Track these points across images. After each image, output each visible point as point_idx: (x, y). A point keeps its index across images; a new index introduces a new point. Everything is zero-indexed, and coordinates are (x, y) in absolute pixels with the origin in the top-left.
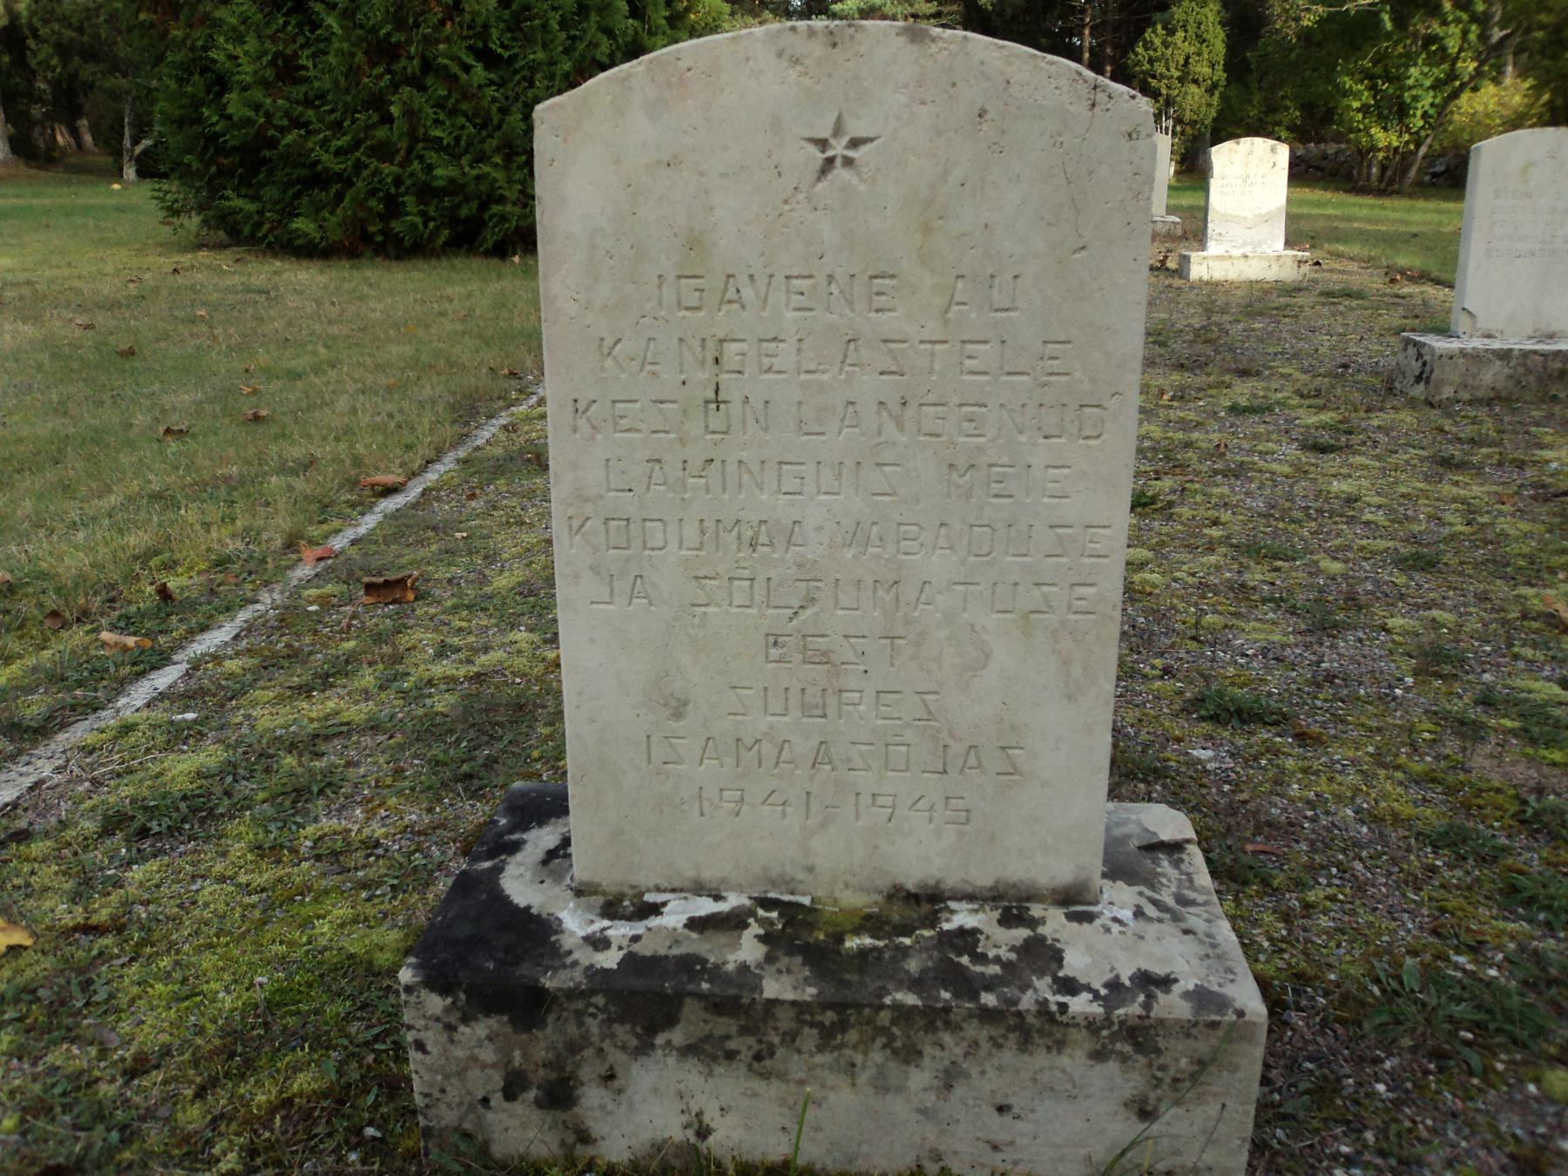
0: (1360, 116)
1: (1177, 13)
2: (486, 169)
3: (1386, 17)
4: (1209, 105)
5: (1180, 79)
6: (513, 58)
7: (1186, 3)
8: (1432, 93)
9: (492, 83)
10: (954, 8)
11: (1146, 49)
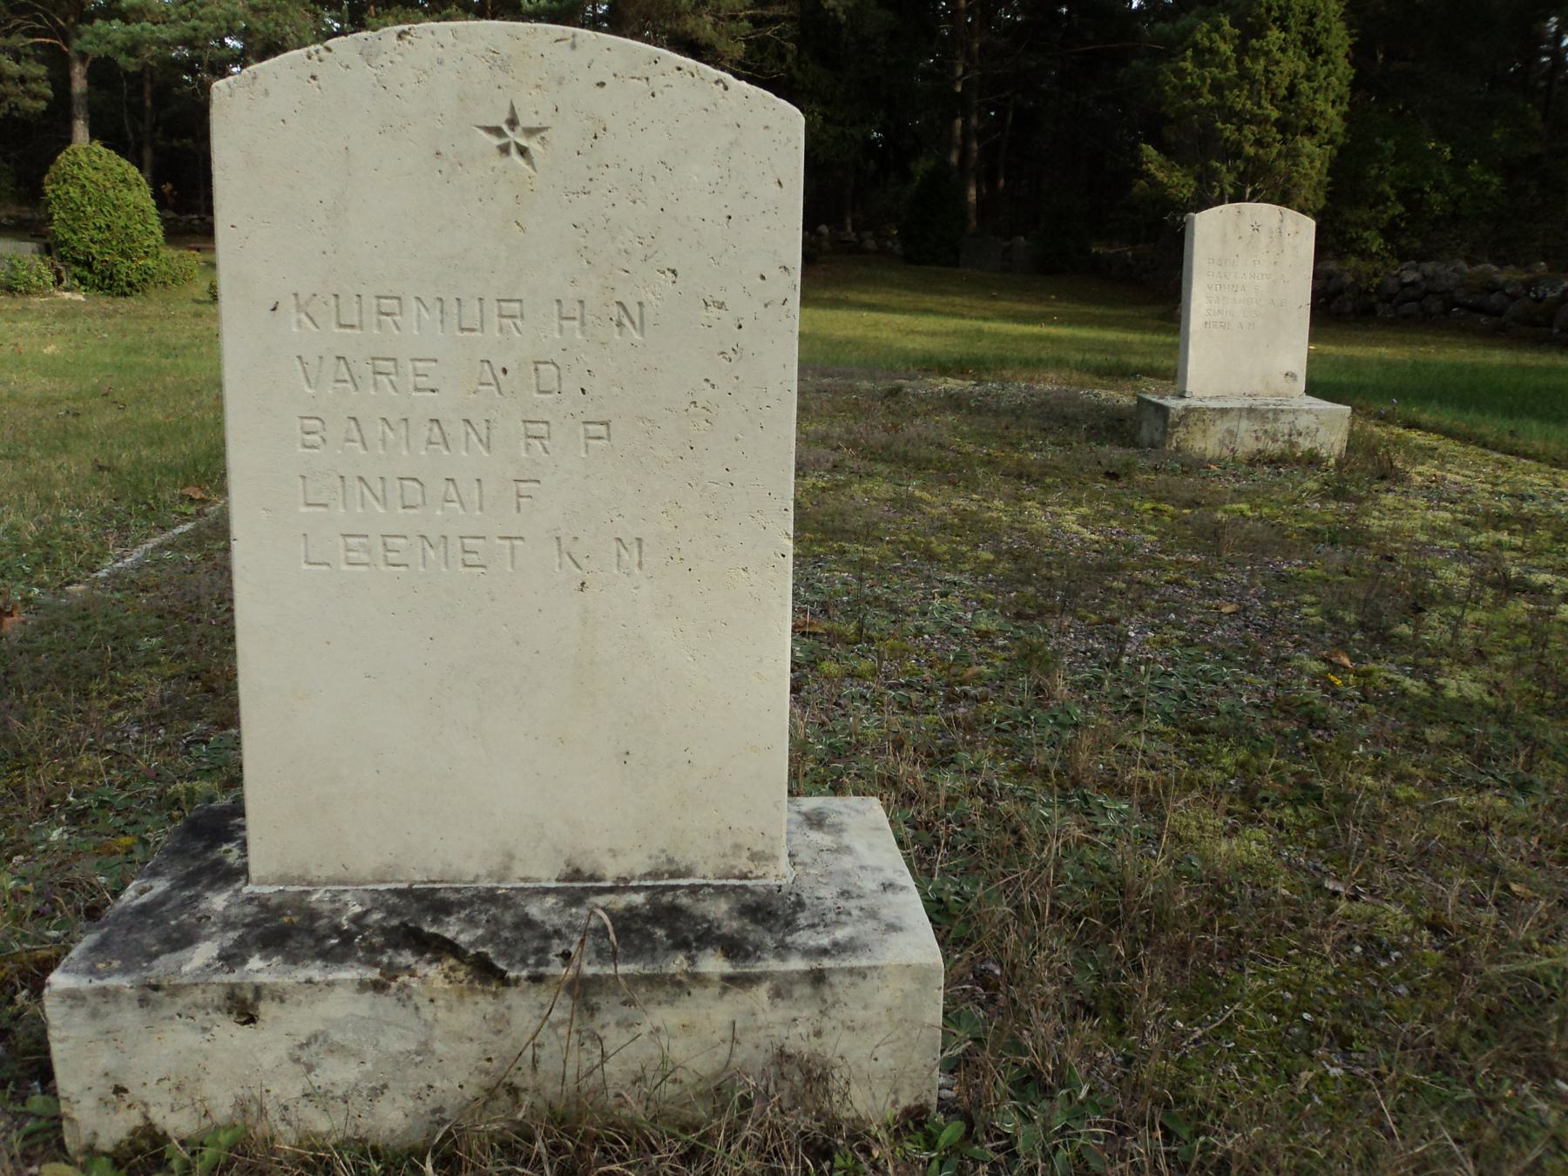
5: (1283, 126)
11: (1202, 65)
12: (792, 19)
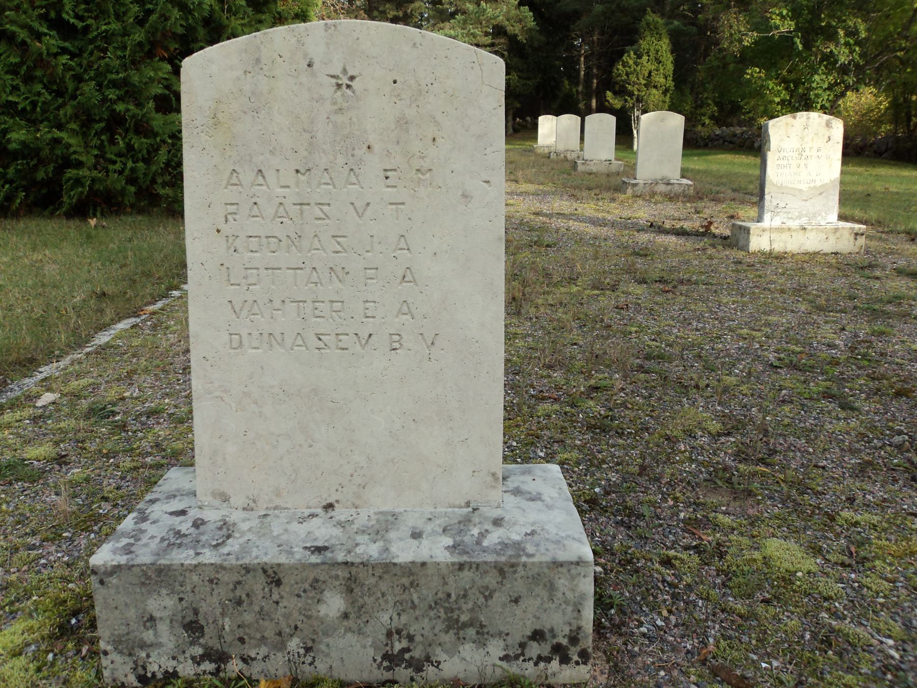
0: (779, 107)
1: (643, 44)
2: (63, 135)
3: (798, 41)
4: (664, 102)
6: (87, 29)
7: (648, 38)
8: (828, 93)
9: (64, 51)
10: (502, 41)
12: (503, 44)
